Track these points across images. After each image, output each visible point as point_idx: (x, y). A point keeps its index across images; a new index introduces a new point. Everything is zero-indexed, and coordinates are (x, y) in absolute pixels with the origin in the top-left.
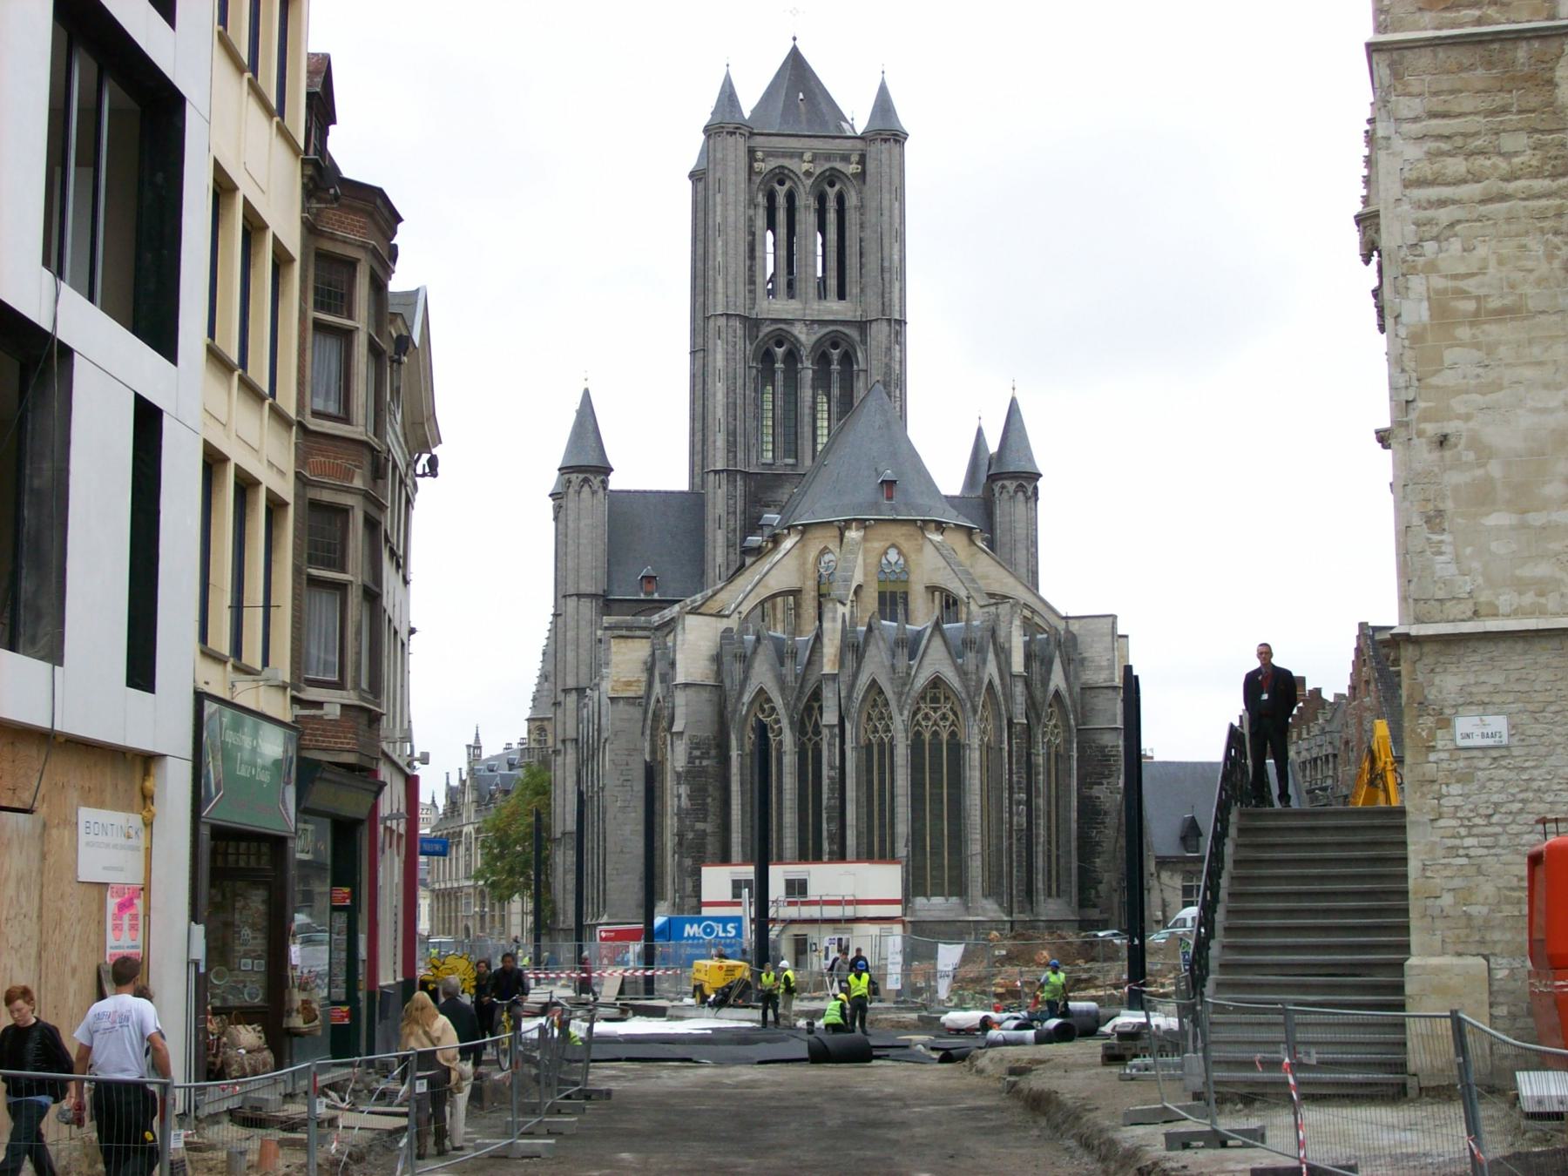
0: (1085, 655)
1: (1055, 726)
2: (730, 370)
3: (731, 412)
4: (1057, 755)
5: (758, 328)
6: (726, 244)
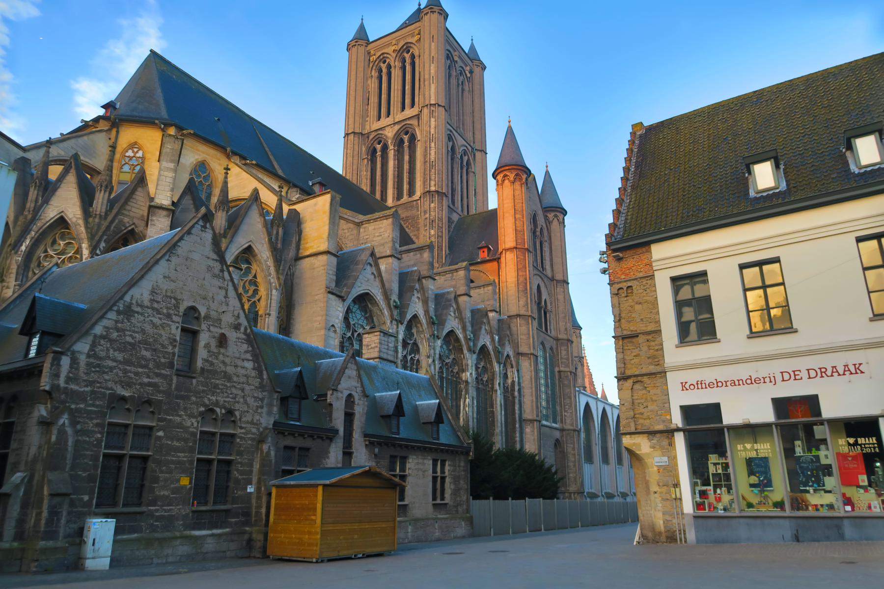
5: (368, 137)
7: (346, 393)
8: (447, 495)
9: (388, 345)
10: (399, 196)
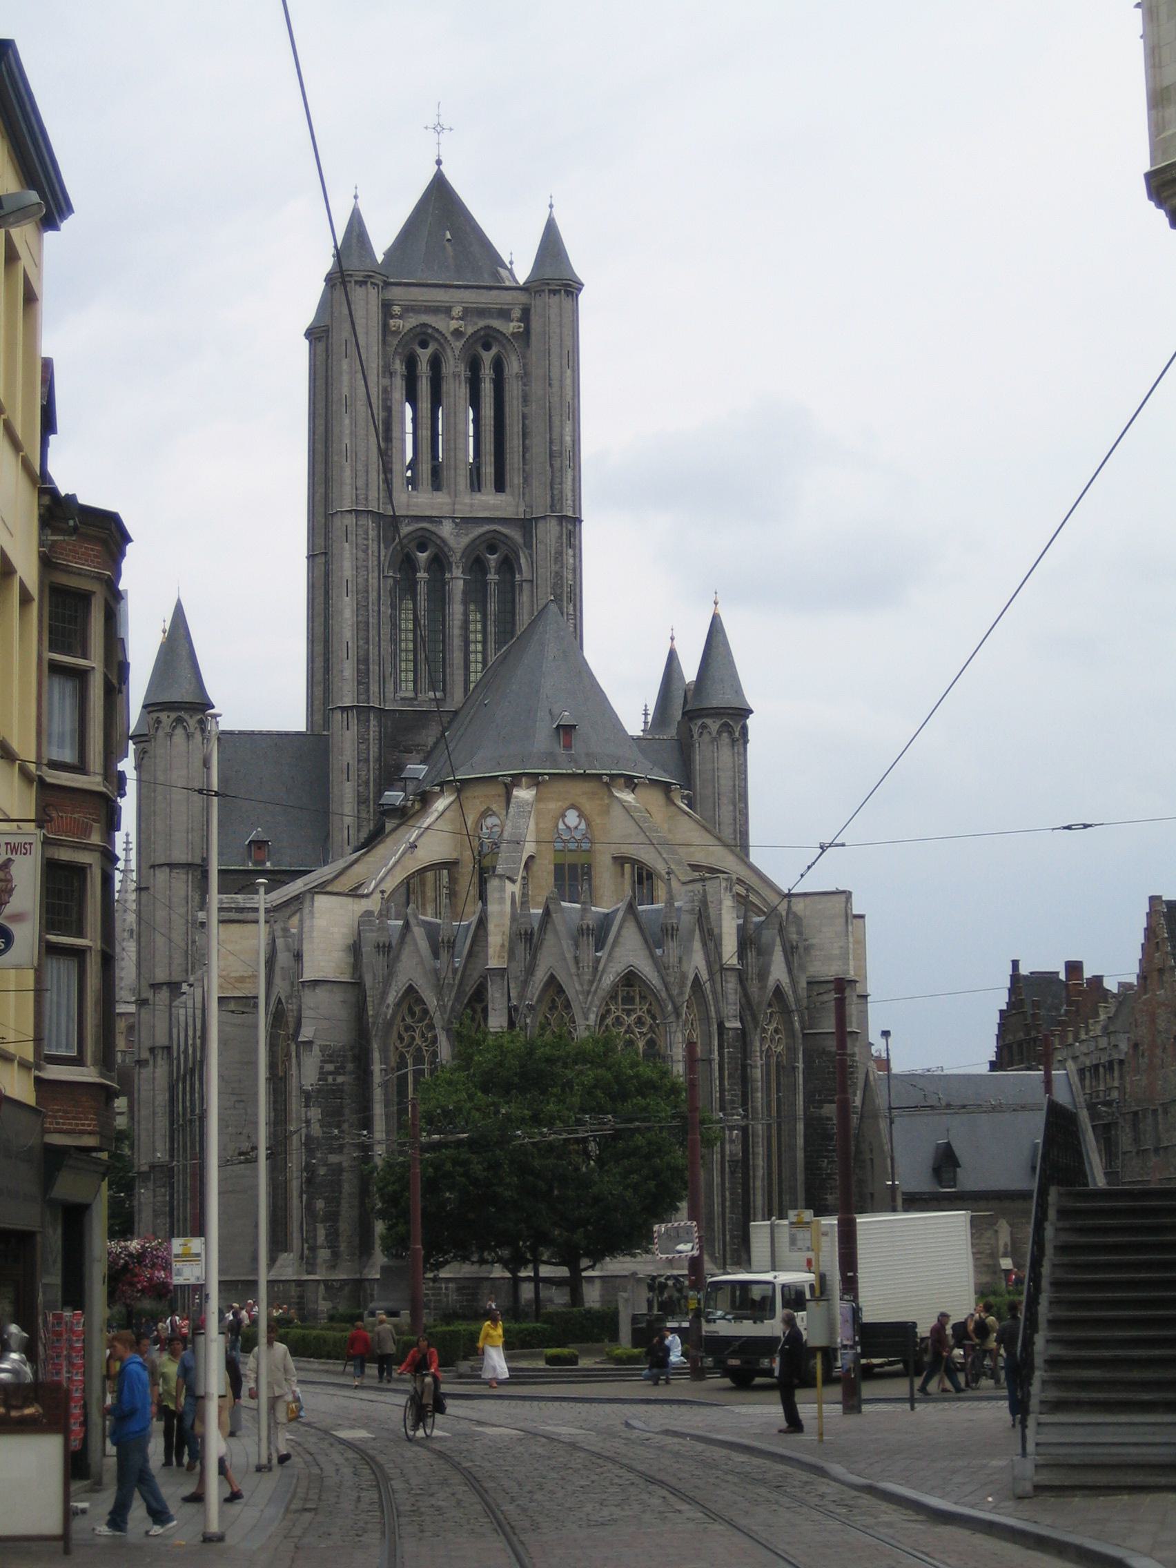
0: (814, 941)
1: (776, 1031)
2: (360, 580)
3: (362, 634)
4: (778, 1064)
6: (354, 422)
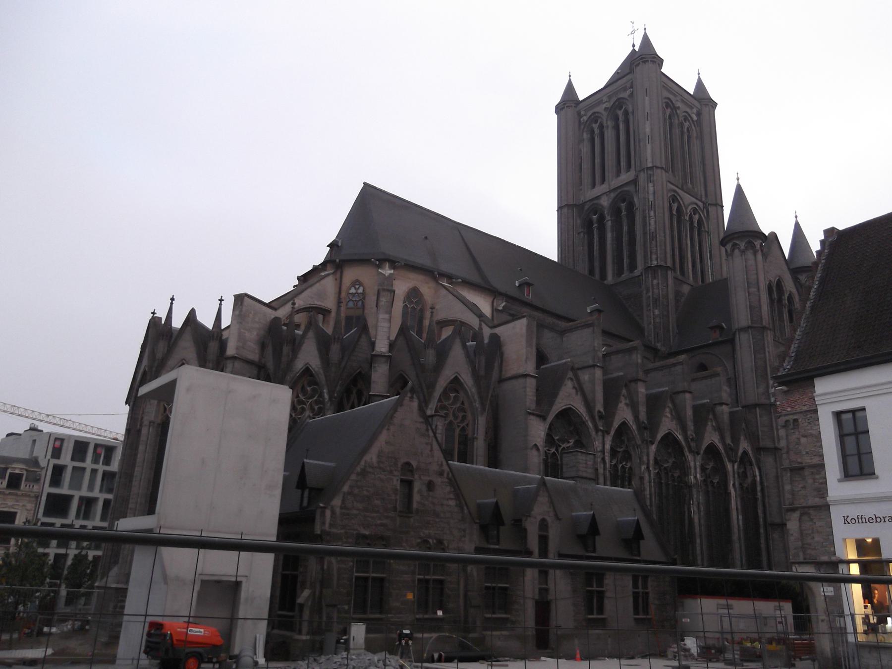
1: (317, 402)
7: (539, 518)
8: (652, 608)
9: (586, 464)
10: (619, 271)
